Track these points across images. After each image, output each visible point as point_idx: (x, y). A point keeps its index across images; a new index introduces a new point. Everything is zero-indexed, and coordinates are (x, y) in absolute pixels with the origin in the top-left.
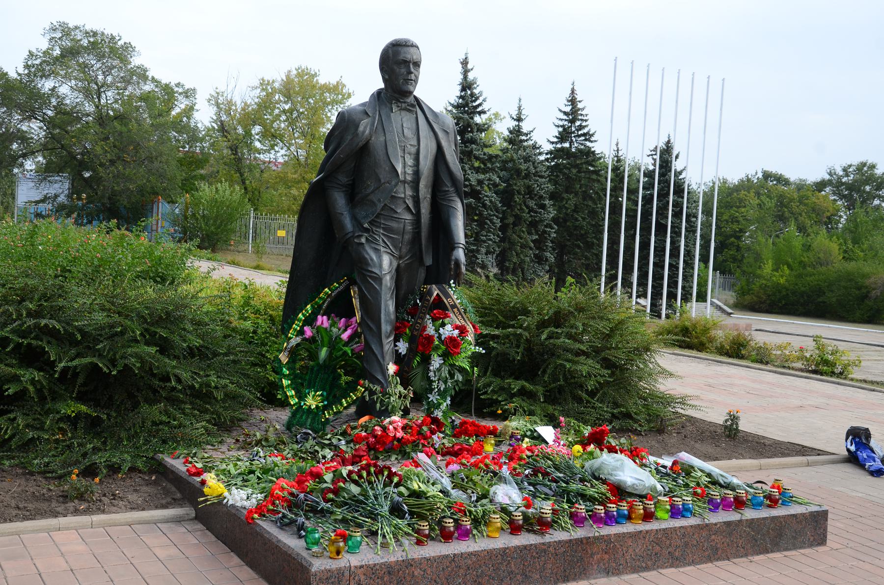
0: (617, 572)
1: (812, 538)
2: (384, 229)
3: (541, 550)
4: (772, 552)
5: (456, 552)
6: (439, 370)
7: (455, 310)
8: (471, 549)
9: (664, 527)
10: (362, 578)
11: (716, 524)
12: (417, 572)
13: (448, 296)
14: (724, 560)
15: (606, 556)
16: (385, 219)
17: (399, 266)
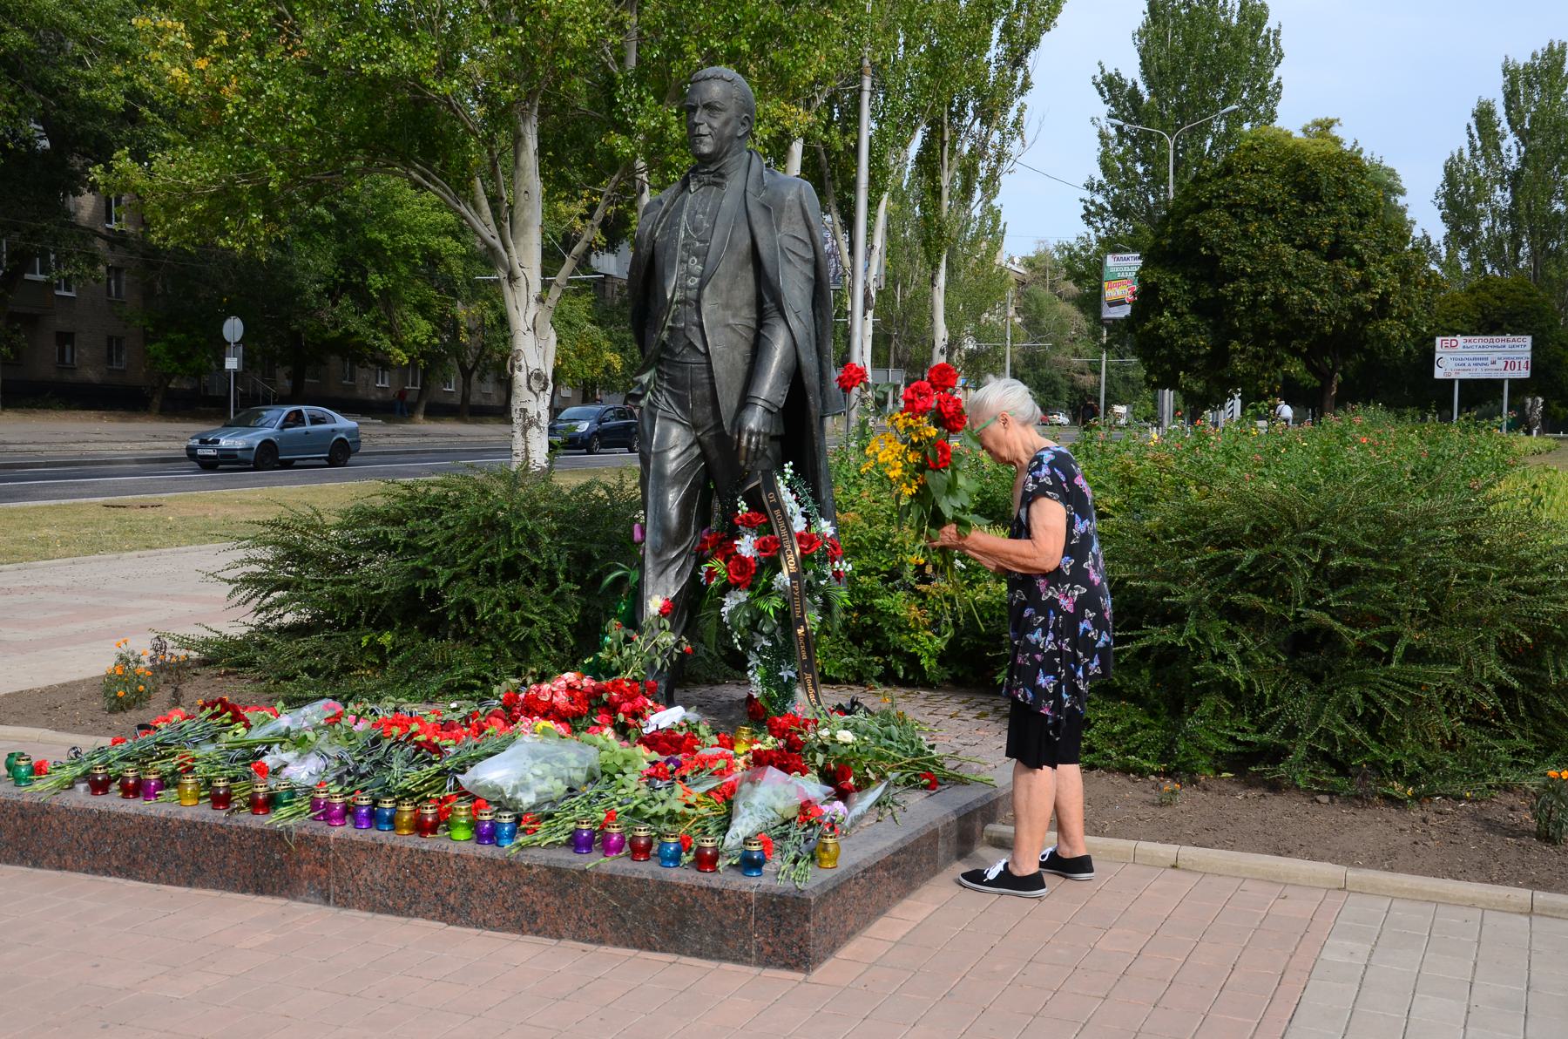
1: (768, 949)
2: (670, 382)
3: (220, 836)
4: (662, 950)
5: (103, 808)
7: (777, 512)
8: (122, 810)
9: (426, 847)
11: (529, 867)
12: (55, 823)
13: (771, 487)
14: (551, 936)
16: (669, 367)
17: (698, 441)
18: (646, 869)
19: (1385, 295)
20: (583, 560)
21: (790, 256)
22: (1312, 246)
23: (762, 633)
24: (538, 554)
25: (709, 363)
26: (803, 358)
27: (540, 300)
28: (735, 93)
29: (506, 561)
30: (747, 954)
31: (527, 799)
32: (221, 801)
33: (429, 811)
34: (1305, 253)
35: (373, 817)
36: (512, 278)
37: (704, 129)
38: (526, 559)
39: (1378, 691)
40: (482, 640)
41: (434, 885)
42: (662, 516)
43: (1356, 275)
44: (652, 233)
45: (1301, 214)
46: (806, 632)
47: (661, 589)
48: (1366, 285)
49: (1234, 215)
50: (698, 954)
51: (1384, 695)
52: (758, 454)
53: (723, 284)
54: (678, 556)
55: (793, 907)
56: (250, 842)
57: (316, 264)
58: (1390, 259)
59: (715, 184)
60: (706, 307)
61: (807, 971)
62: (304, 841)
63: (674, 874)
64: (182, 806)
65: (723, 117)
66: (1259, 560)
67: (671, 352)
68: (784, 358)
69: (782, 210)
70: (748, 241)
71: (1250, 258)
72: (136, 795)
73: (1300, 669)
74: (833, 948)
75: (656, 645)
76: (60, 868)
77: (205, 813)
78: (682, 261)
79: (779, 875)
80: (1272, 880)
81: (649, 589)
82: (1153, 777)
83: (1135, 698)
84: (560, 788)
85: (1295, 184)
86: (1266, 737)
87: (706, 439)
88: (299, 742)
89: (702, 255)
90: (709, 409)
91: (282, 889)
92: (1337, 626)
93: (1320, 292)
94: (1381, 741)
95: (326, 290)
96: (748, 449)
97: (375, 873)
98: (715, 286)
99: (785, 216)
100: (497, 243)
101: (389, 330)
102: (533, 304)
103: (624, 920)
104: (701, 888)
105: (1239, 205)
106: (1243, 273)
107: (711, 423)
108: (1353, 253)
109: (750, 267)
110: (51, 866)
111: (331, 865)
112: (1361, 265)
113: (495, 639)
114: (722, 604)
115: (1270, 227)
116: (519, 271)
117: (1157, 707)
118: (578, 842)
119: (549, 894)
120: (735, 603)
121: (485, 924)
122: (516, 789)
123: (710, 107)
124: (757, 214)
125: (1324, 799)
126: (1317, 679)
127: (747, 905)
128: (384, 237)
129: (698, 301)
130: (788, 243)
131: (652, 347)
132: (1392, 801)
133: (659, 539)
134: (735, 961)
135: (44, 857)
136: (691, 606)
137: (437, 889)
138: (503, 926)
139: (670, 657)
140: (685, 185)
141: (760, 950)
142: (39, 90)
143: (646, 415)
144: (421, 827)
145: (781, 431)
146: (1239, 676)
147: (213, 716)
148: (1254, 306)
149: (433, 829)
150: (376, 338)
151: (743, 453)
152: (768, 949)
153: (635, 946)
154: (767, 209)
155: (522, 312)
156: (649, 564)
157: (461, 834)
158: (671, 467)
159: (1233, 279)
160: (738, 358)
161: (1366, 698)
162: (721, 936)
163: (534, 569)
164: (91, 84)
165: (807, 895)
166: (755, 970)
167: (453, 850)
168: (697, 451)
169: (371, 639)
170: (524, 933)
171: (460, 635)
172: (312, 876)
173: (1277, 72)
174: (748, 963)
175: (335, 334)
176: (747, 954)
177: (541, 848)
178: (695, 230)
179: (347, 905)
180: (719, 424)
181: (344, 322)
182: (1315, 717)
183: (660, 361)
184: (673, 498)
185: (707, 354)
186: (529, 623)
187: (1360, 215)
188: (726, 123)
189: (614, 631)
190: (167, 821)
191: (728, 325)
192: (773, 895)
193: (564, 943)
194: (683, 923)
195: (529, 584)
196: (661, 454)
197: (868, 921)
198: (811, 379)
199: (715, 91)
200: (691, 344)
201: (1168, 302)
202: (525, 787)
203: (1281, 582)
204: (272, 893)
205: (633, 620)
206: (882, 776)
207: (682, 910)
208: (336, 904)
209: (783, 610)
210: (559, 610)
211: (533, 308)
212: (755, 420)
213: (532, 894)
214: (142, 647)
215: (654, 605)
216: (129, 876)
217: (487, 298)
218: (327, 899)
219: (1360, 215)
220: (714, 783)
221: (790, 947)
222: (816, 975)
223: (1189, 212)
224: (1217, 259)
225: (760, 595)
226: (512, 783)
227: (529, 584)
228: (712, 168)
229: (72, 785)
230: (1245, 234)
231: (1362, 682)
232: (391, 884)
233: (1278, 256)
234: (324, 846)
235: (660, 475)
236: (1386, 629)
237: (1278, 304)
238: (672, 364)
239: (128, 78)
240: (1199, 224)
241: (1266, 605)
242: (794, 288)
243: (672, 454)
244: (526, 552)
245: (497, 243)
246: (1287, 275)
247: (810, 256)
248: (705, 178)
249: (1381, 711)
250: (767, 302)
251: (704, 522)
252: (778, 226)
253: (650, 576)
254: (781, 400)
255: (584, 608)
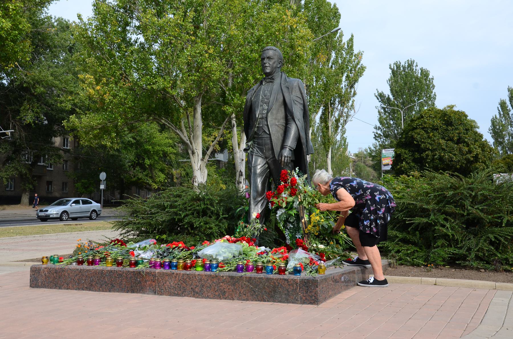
0: (161, 293)
1: (304, 298)
3: (120, 275)
4: (268, 301)
6: (280, 216)
9: (188, 273)
10: (46, 273)
11: (223, 277)
12: (66, 274)
14: (230, 299)
15: (154, 283)
16: (257, 139)
17: (267, 163)
18: (262, 275)
19: (477, 154)
20: (228, 210)
21: (296, 102)
22: (451, 140)
23: (290, 222)
24: (214, 207)
25: (271, 137)
26: (301, 134)
27: (202, 160)
28: (277, 53)
29: (204, 208)
30: (297, 300)
31: (220, 259)
32: (120, 264)
33: (189, 261)
34: (449, 142)
35: (170, 266)
36: (193, 153)
37: (267, 65)
38: (210, 209)
39: (499, 235)
40: (196, 235)
41: (191, 285)
42: (256, 186)
43: (467, 149)
44: (251, 99)
45: (447, 130)
46: (305, 221)
47: (256, 210)
48: (470, 152)
49: (425, 131)
50: (280, 302)
51: (500, 236)
52: (287, 164)
53: (275, 112)
54: (261, 200)
55: (312, 283)
56: (130, 276)
57: (129, 157)
58: (477, 143)
59: (271, 82)
60: (269, 119)
61: (317, 304)
62: (147, 273)
63: (271, 276)
64: (108, 267)
65: (273, 61)
66: (454, 195)
67: (258, 134)
68: (295, 133)
69: (293, 88)
70: (282, 98)
71: (431, 144)
72: (92, 265)
73: (470, 232)
74: (325, 299)
75: (255, 228)
76: (68, 289)
77: (115, 268)
78: (261, 106)
79: (305, 275)
80: (470, 287)
81: (252, 210)
82: (423, 267)
83: (414, 244)
84: (230, 256)
85: (444, 120)
86: (461, 251)
87: (269, 162)
88: (144, 249)
89: (268, 104)
90: (270, 152)
91: (140, 290)
92: (482, 215)
93: (455, 155)
94: (500, 253)
95: (132, 165)
96: (284, 162)
97: (171, 283)
98: (272, 113)
99: (294, 91)
100: (188, 142)
101: (151, 177)
102: (200, 161)
103: (255, 292)
104: (281, 279)
105: (425, 128)
106: (428, 149)
107: (271, 156)
108: (464, 142)
109: (283, 106)
110: (65, 288)
111: (156, 281)
112: (468, 145)
113: (200, 234)
114: (277, 213)
115: (436, 134)
116: (195, 151)
117: (422, 246)
118: (238, 269)
119: (229, 285)
120: (281, 213)
121: (208, 297)
122: (217, 255)
123: (269, 58)
124: (285, 90)
125: (483, 270)
126: (475, 235)
127: (296, 283)
128: (150, 147)
129: (267, 118)
130: (295, 98)
131: (251, 133)
132: (506, 271)
133: (255, 194)
134: (293, 303)
135: (63, 286)
136: (266, 215)
137: (192, 287)
138: (214, 297)
139: (260, 232)
140: (261, 83)
141: (301, 298)
142: (45, 105)
143: (250, 155)
144: (186, 267)
145: (294, 159)
146: (450, 233)
147: (114, 245)
148: (433, 160)
149: (190, 267)
150: (147, 180)
151: (283, 163)
152: (304, 298)
153: (259, 301)
154: (288, 88)
155: (196, 164)
156: (252, 202)
157: (199, 269)
158: (258, 171)
159: (425, 151)
160: (280, 135)
161: (495, 238)
162: (288, 295)
163: (212, 212)
164: (61, 102)
165: (317, 279)
166: (300, 305)
167: (197, 273)
168: (267, 166)
169: (159, 237)
170: (221, 299)
171: (189, 233)
172: (150, 285)
173: (434, 91)
174: (297, 303)
175: (134, 179)
176: (297, 300)
177: (226, 272)
178: (265, 96)
179: (161, 294)
180: (274, 157)
181: (137, 175)
182: (477, 245)
183: (254, 138)
184: (259, 181)
185: (270, 134)
186: (211, 228)
187: (466, 130)
188: (274, 63)
189: (241, 223)
190: (102, 270)
191: (276, 125)
192: (305, 280)
193: (234, 301)
194: (275, 291)
195: (210, 217)
196: (255, 166)
197: (335, 294)
198: (304, 141)
199: (271, 53)
200: (265, 131)
201: (404, 159)
202: (220, 255)
203: (461, 203)
204: (137, 292)
205: (247, 221)
206: (335, 257)
207: (274, 287)
208: (158, 294)
209: (297, 214)
210: (221, 224)
211: (200, 162)
212: (286, 153)
213: (224, 286)
214: (86, 243)
215: (254, 215)
216: (90, 290)
217: (182, 167)
218: (155, 293)
219: (466, 130)
220: (280, 256)
221: (311, 297)
222: (320, 306)
223: (410, 130)
224: (420, 145)
225: (289, 210)
226: (215, 253)
227: (210, 217)
228: (270, 77)
229: (71, 264)
230: (429, 137)
231: (492, 233)
232: (176, 286)
233: (440, 143)
234: (154, 275)
235: (255, 173)
236: (499, 215)
237: (441, 159)
238: (258, 138)
239: (73, 100)
240: (413, 134)
241: (458, 211)
242: (298, 112)
243: (259, 167)
244: (209, 207)
245: (188, 142)
246: (443, 149)
247: (302, 102)
248: (268, 80)
249: (500, 241)
250: (289, 116)
251: (269, 189)
252: (292, 93)
253: (252, 206)
254: (294, 146)
255: (229, 225)
